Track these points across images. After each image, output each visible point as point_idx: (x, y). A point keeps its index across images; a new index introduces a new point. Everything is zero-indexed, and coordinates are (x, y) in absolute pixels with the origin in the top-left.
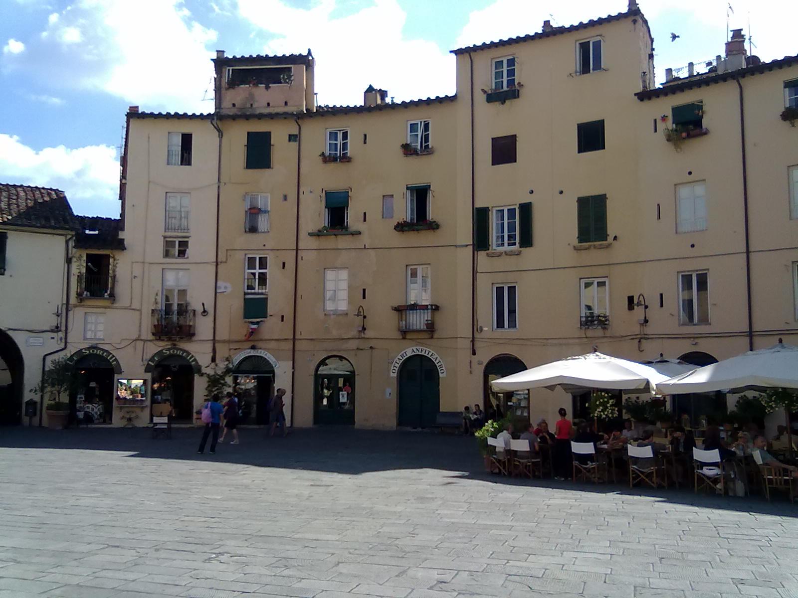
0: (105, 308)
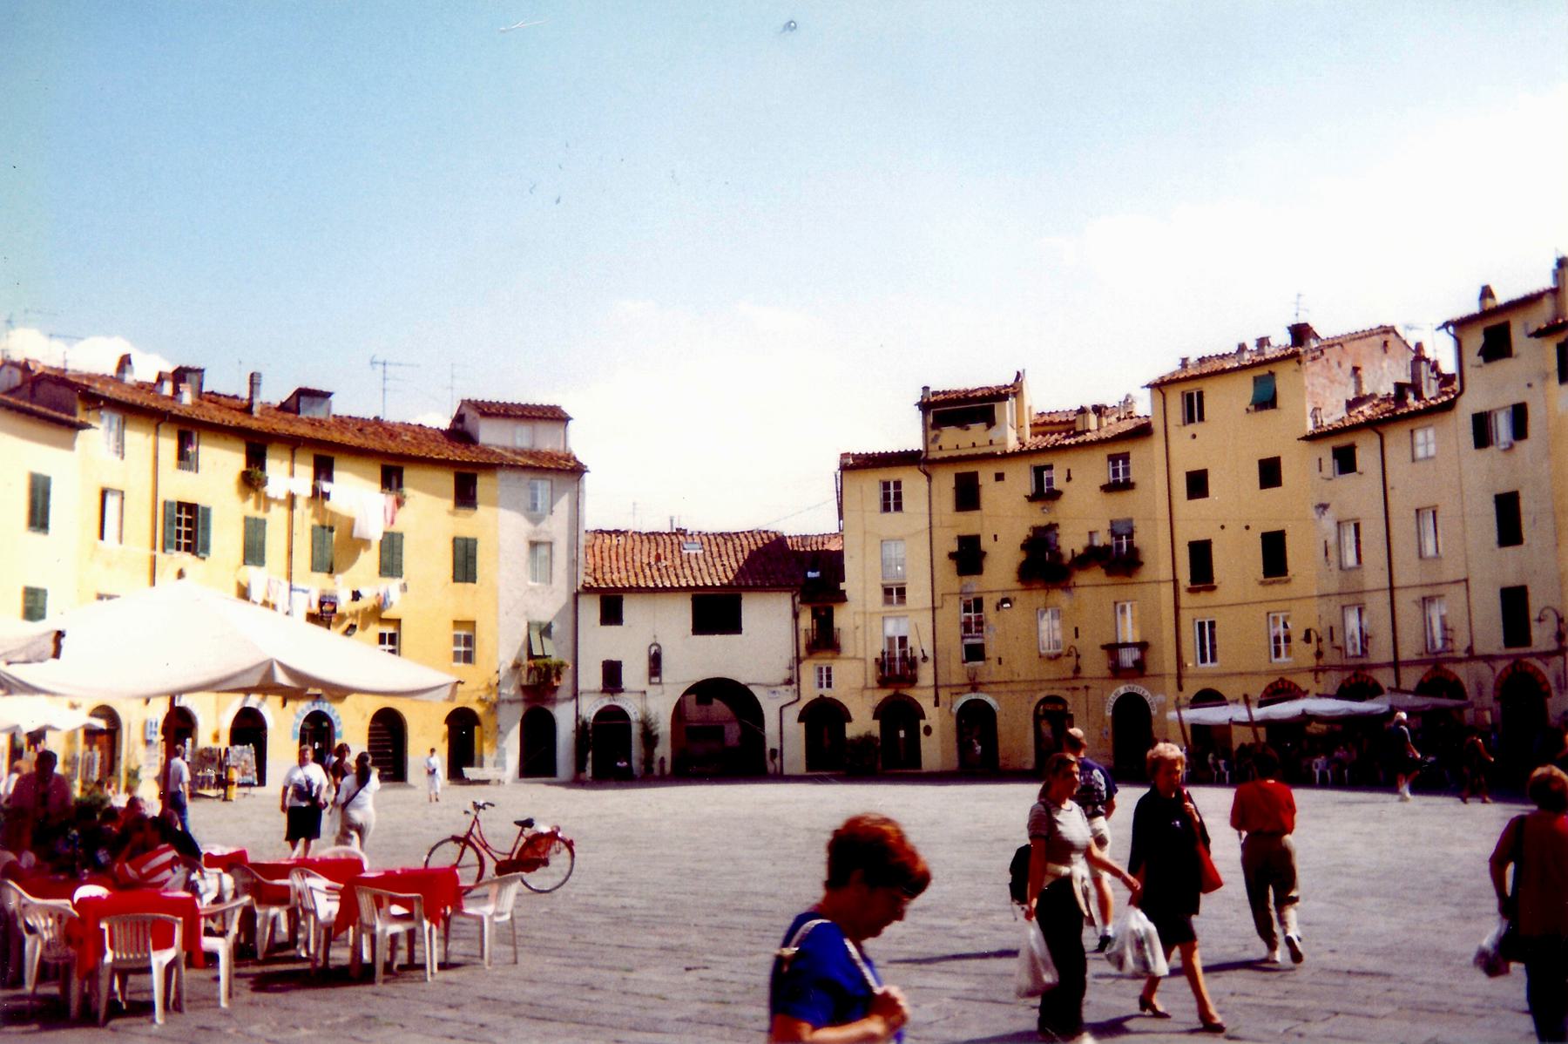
0: (833, 658)
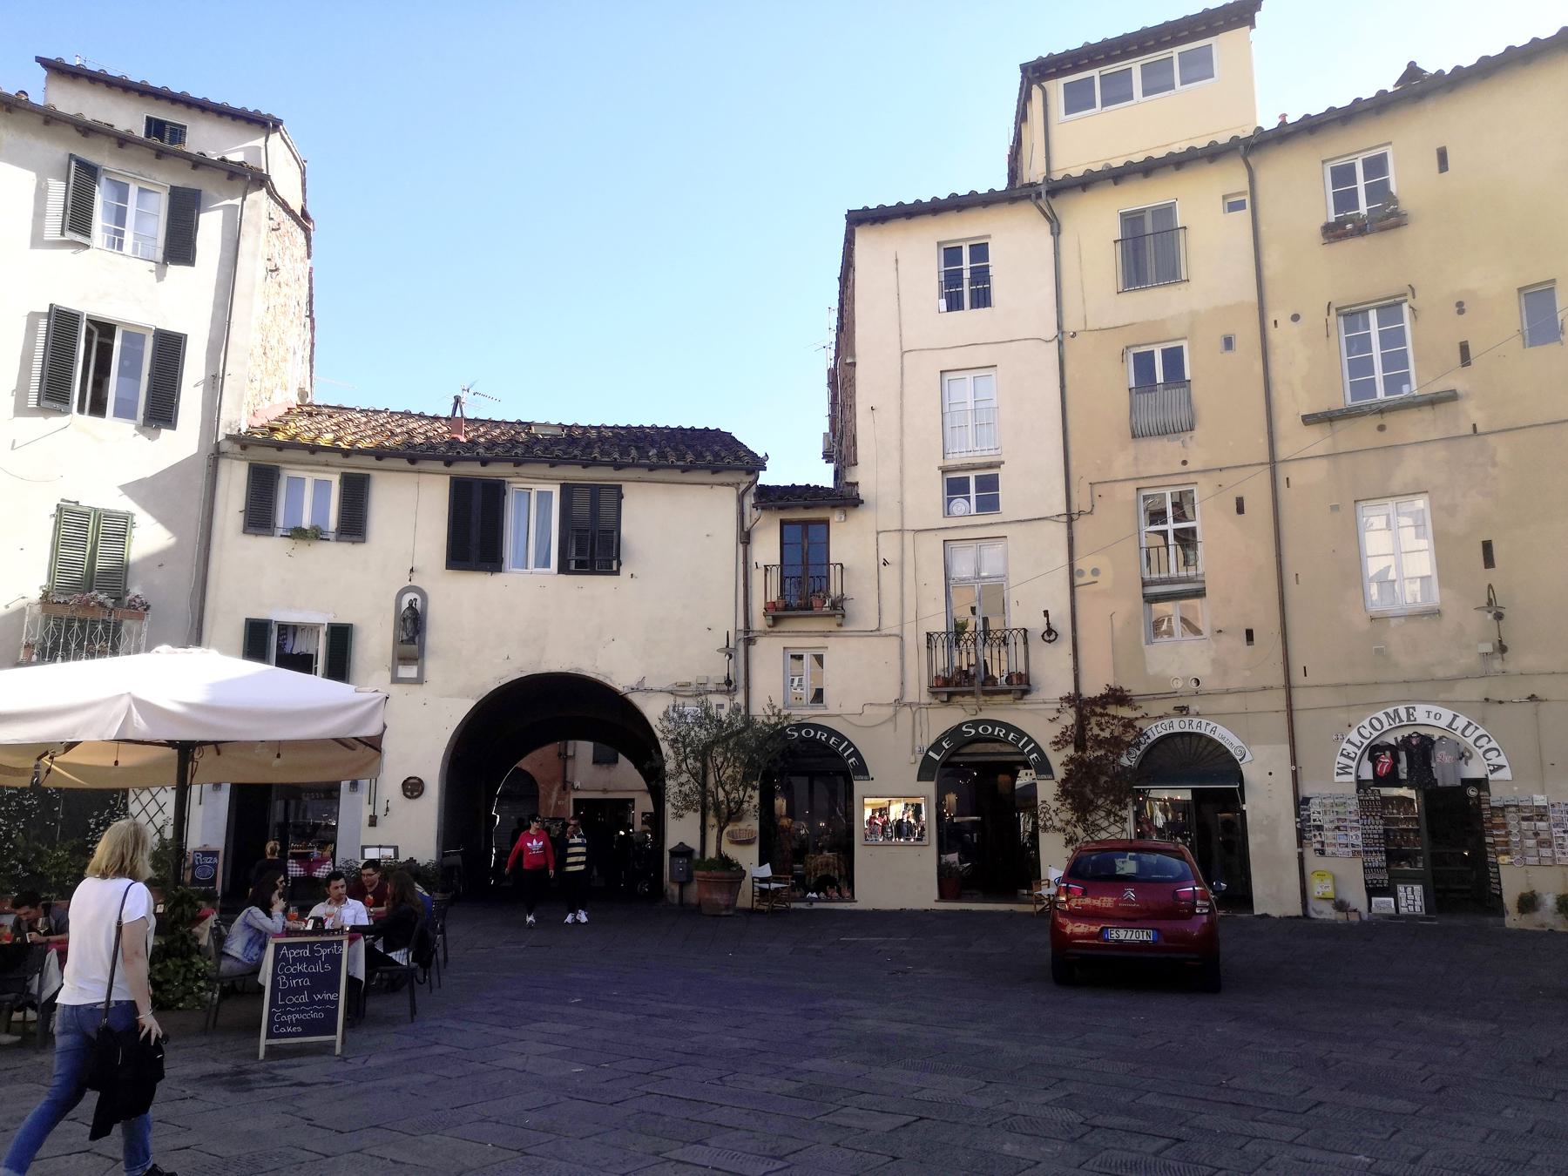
0: (826, 634)
